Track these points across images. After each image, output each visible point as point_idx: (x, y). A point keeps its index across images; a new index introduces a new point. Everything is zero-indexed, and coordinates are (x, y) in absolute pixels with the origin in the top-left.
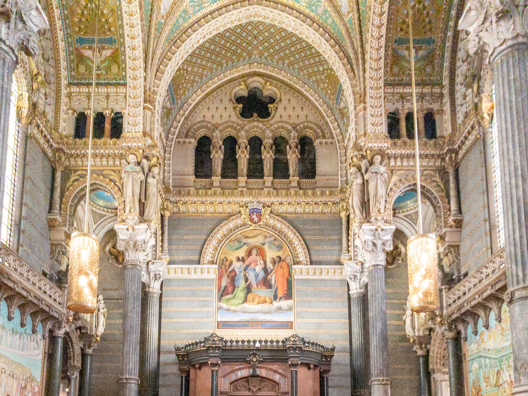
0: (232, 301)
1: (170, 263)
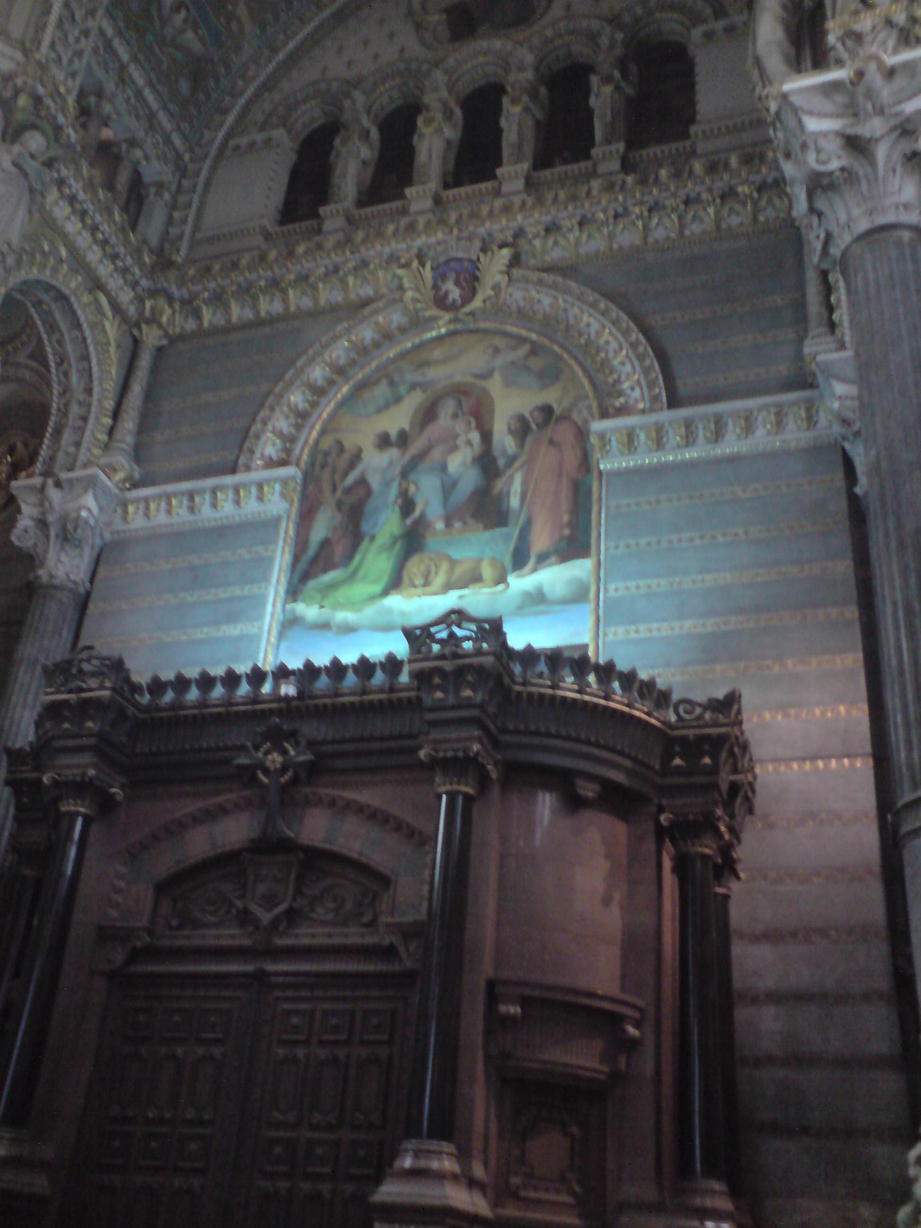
0: (343, 593)
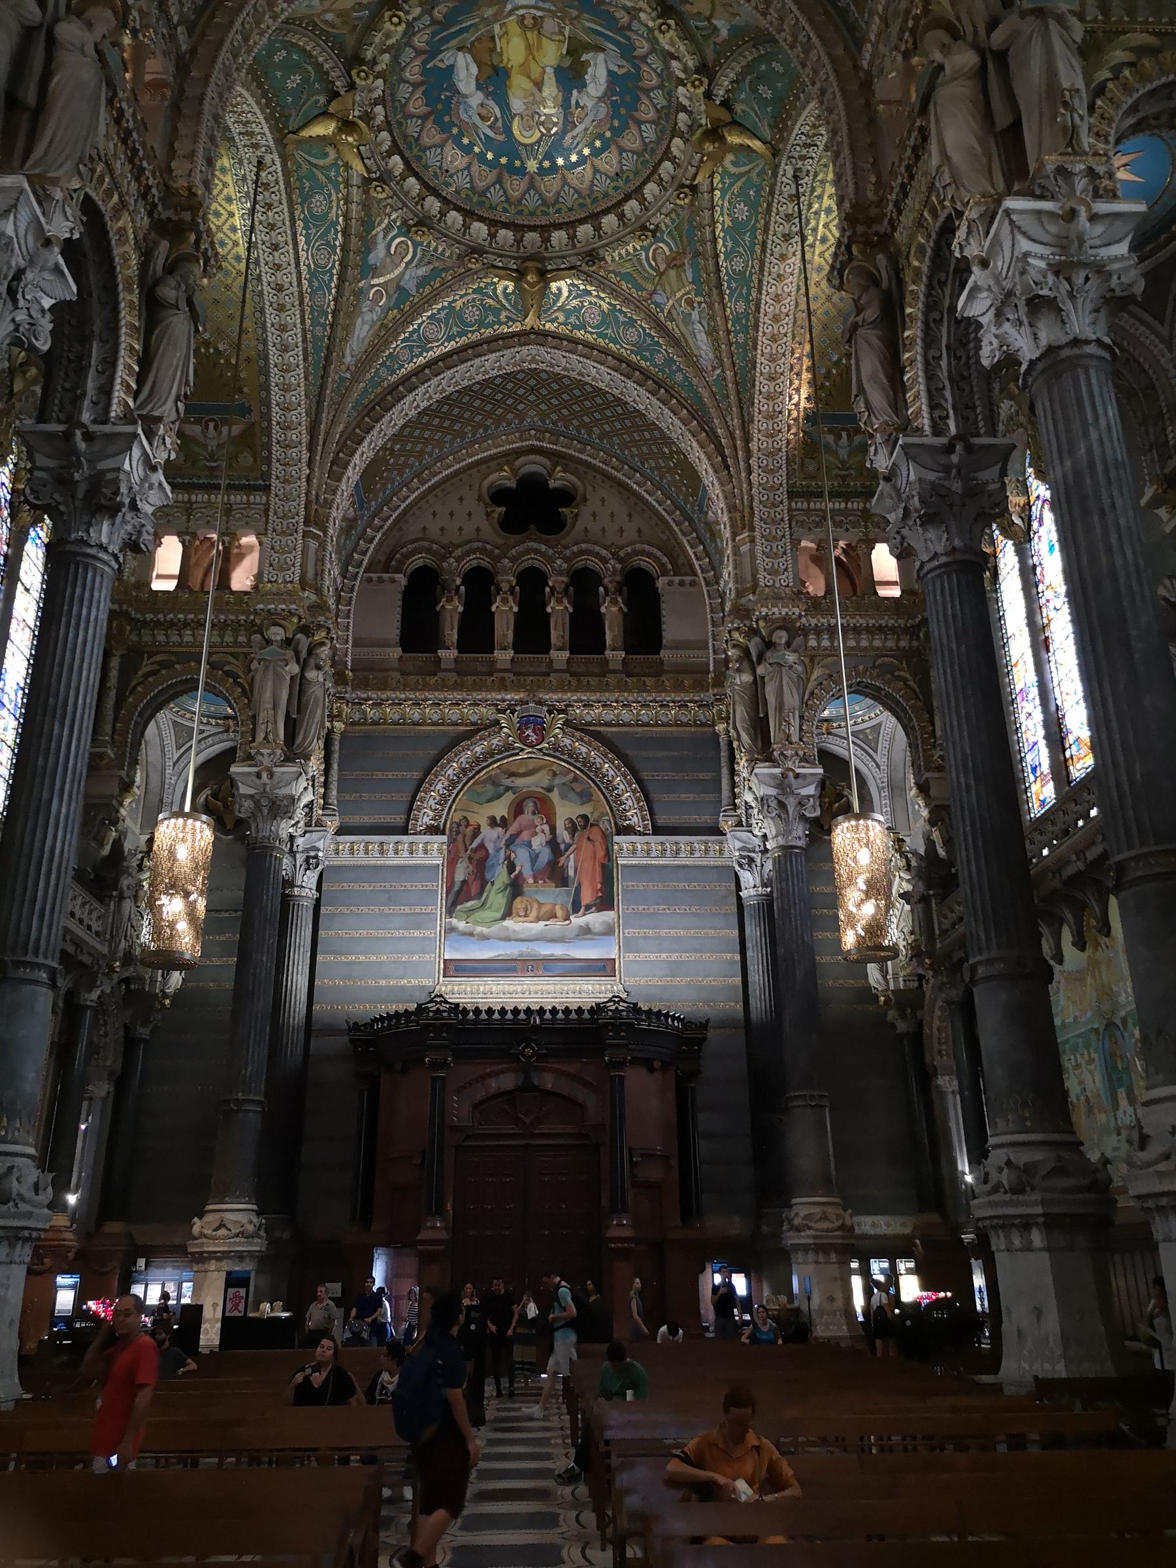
0: (479, 915)
1: (340, 831)
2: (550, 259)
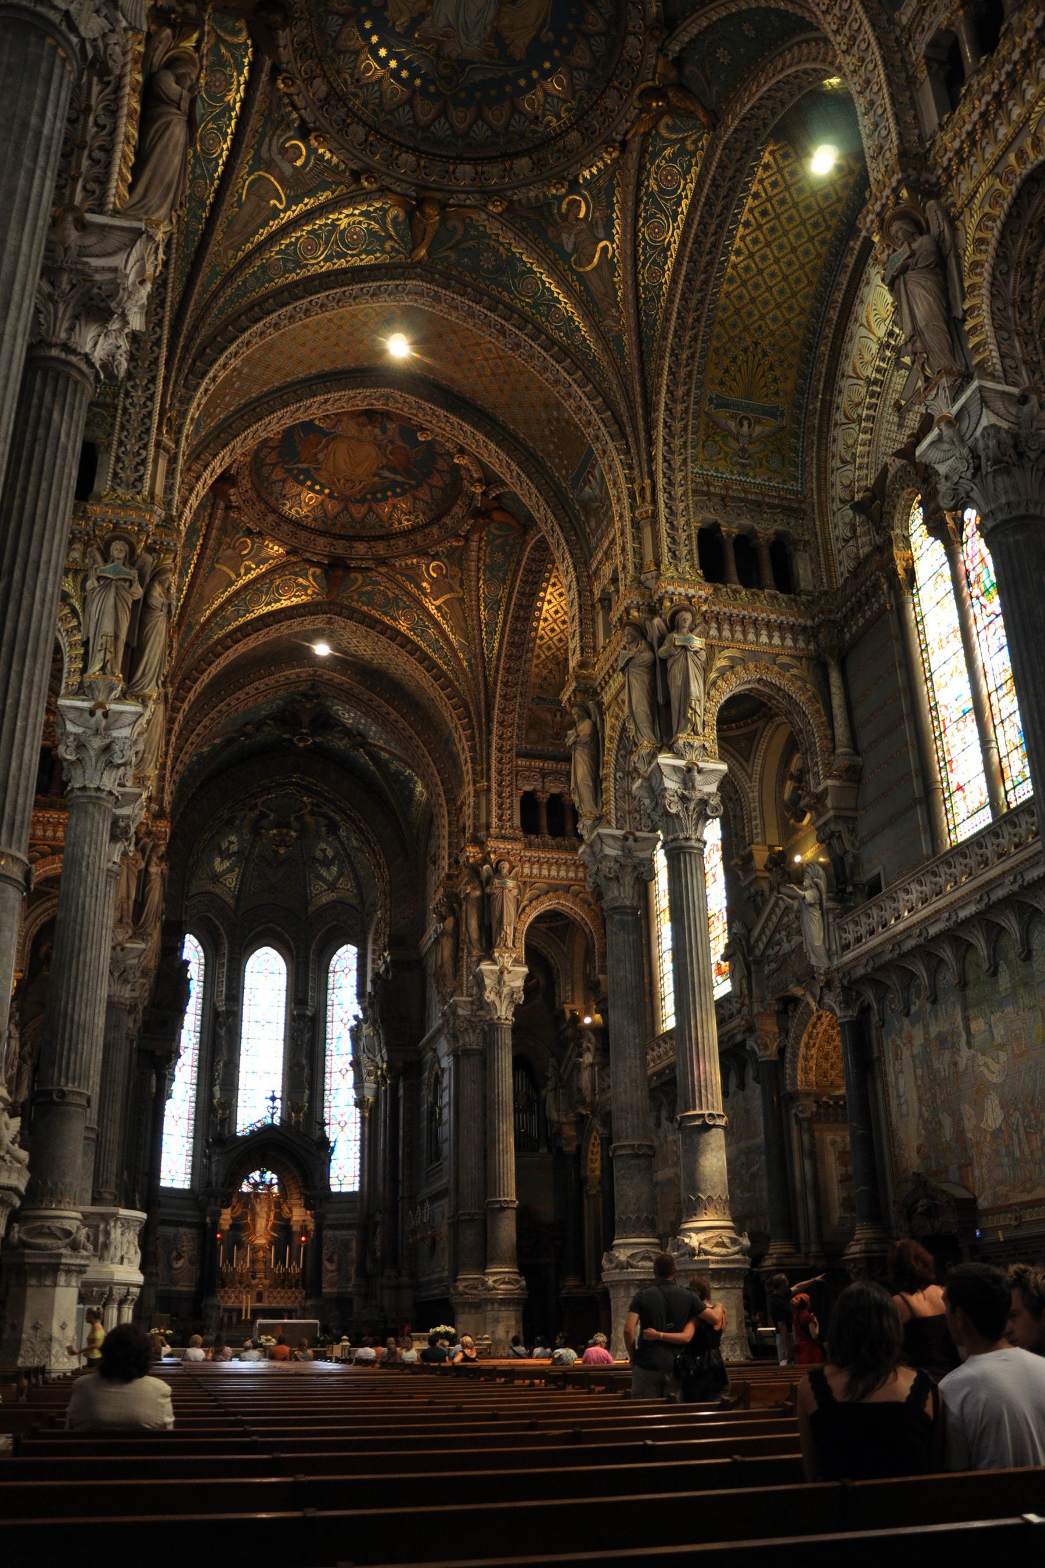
2: (454, 192)
